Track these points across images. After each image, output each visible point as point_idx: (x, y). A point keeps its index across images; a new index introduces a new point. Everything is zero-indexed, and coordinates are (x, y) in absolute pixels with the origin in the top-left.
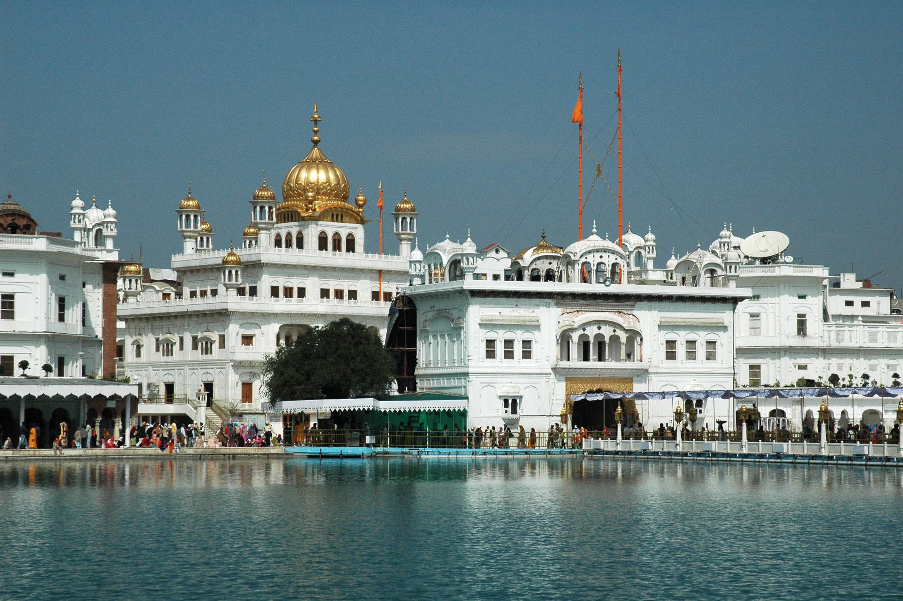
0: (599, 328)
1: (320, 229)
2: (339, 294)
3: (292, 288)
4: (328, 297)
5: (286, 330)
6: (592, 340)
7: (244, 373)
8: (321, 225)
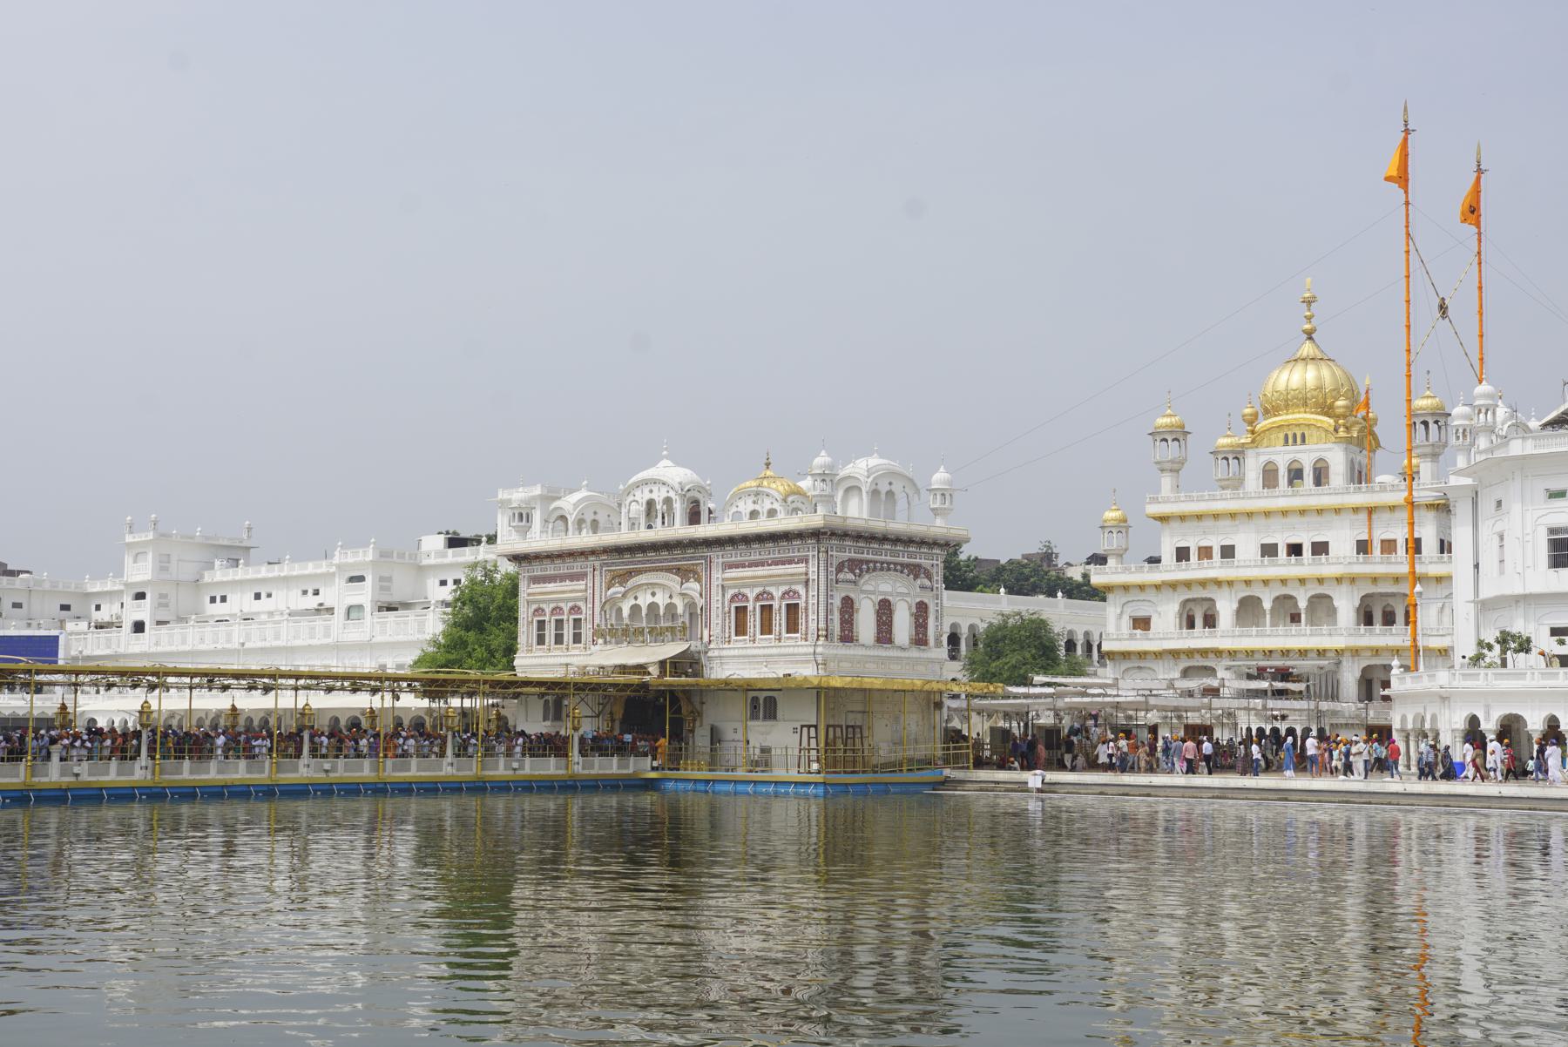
0: (653, 594)
1: (1263, 459)
2: (1295, 550)
3: (1211, 548)
4: (1188, 559)
5: (1205, 608)
7: (1127, 670)
8: (1264, 454)
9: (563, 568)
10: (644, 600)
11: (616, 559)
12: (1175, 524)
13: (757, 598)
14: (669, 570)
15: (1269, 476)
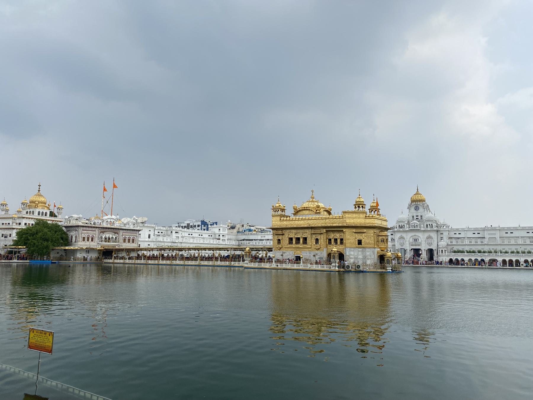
0: (109, 235)
1: (38, 211)
6: (107, 238)
9: (90, 229)
10: (107, 236)
11: (102, 229)
12: (25, 219)
13: (128, 238)
14: (112, 232)
15: (39, 214)
